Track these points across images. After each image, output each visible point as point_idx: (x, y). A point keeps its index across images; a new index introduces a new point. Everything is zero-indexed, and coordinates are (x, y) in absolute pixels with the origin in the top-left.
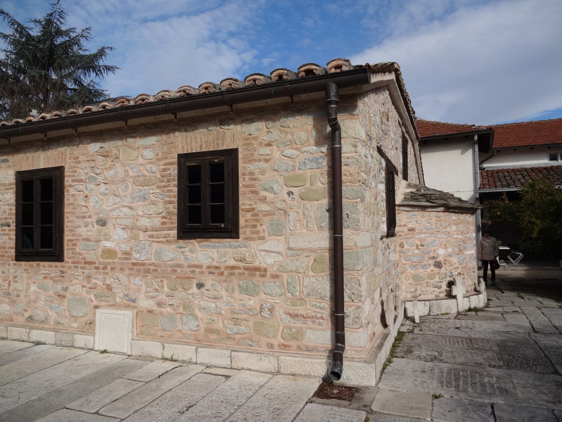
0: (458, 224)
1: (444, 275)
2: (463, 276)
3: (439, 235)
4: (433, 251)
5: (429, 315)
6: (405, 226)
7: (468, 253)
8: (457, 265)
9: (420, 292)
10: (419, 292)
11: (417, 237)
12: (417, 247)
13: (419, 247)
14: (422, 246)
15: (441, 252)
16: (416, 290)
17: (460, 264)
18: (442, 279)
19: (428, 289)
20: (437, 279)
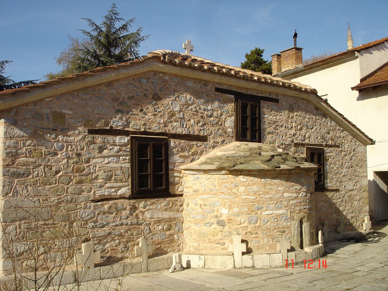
0: (249, 186)
1: (228, 233)
2: (256, 236)
3: (222, 196)
4: (216, 210)
5: (204, 267)
6: (190, 187)
7: (267, 213)
8: (246, 224)
9: (202, 247)
10: (201, 247)
11: (200, 197)
12: (201, 207)
13: (203, 207)
14: (204, 205)
15: (225, 211)
16: (199, 245)
17: (250, 224)
18: (225, 236)
19: (209, 245)
20: (219, 237)
